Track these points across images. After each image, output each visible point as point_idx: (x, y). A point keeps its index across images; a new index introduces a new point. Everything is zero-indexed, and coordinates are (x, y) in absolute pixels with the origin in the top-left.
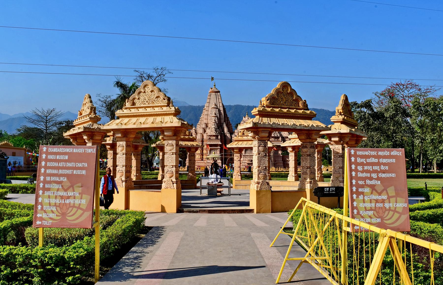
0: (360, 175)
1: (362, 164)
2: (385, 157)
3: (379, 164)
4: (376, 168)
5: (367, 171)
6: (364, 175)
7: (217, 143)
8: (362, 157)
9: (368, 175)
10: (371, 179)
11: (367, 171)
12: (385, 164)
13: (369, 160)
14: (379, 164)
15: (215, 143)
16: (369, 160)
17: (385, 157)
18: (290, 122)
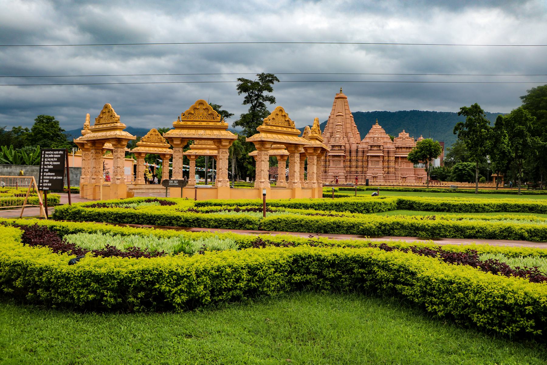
0: (46, 163)
1: (47, 158)
2: (56, 154)
3: (53, 158)
4: (52, 159)
5: (49, 161)
6: (48, 163)
7: (340, 154)
8: (47, 154)
9: (48, 163)
10: (49, 165)
11: (49, 161)
12: (56, 158)
13: (50, 156)
14: (53, 158)
15: (337, 154)
16: (50, 156)
17: (56, 154)
18: (201, 133)
